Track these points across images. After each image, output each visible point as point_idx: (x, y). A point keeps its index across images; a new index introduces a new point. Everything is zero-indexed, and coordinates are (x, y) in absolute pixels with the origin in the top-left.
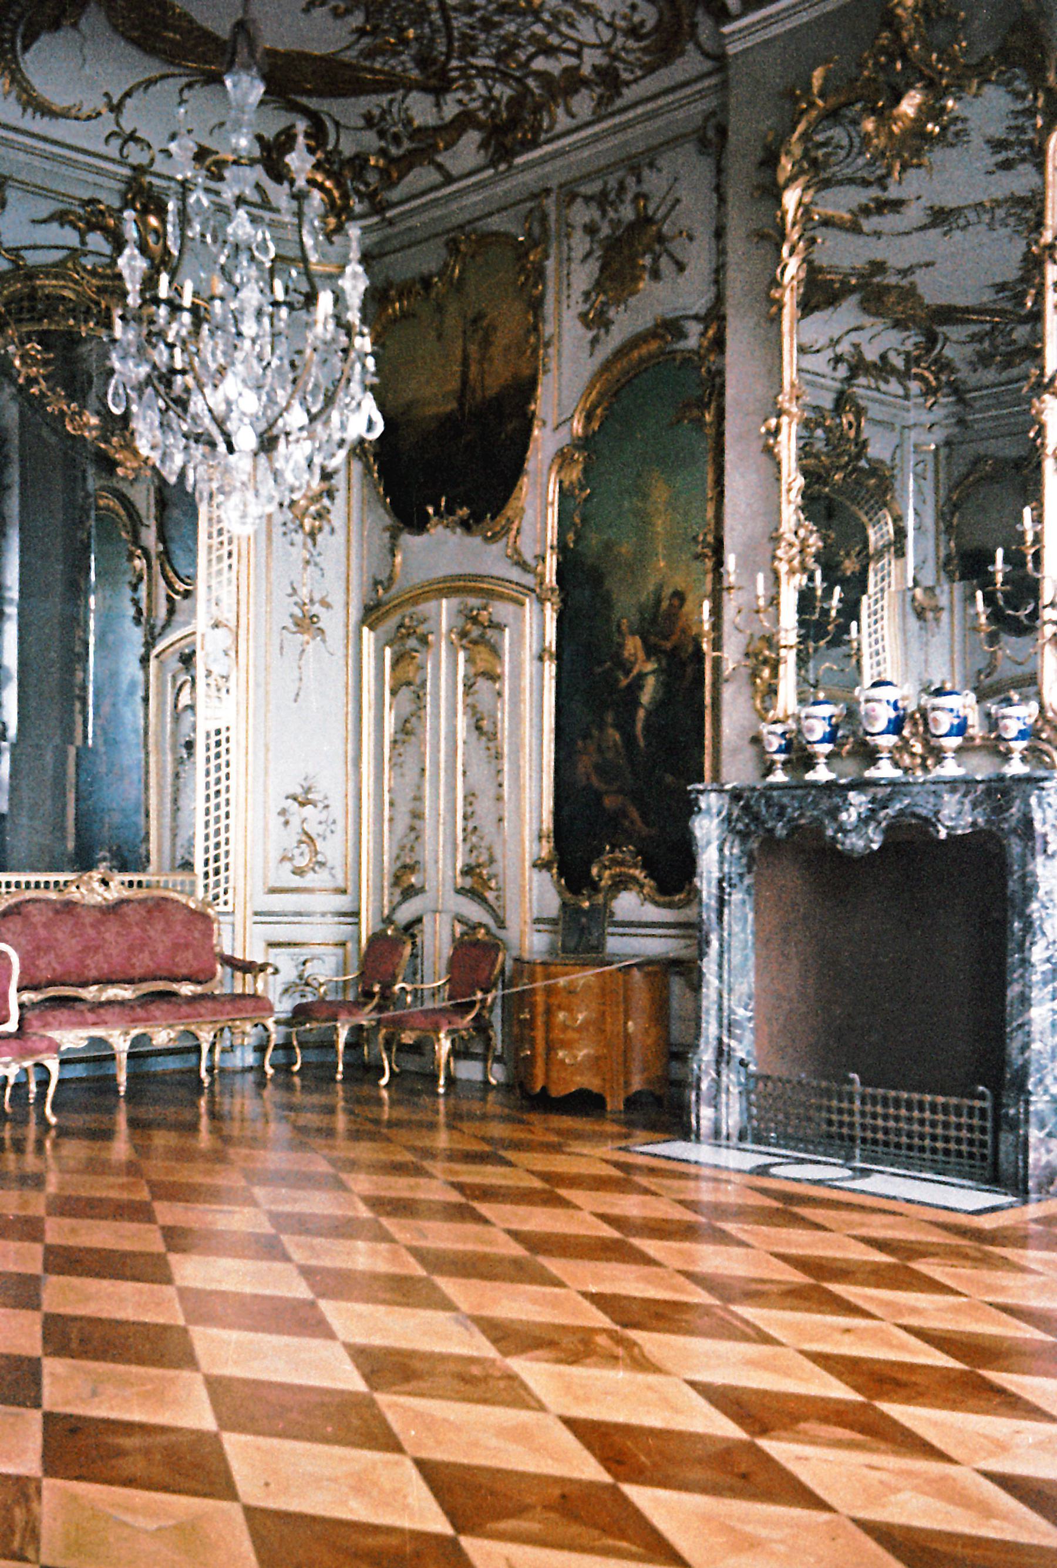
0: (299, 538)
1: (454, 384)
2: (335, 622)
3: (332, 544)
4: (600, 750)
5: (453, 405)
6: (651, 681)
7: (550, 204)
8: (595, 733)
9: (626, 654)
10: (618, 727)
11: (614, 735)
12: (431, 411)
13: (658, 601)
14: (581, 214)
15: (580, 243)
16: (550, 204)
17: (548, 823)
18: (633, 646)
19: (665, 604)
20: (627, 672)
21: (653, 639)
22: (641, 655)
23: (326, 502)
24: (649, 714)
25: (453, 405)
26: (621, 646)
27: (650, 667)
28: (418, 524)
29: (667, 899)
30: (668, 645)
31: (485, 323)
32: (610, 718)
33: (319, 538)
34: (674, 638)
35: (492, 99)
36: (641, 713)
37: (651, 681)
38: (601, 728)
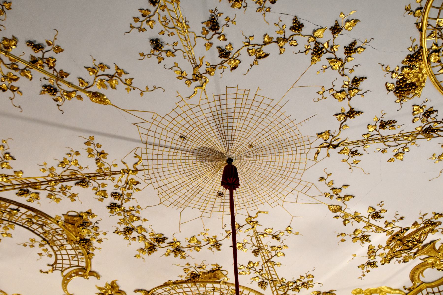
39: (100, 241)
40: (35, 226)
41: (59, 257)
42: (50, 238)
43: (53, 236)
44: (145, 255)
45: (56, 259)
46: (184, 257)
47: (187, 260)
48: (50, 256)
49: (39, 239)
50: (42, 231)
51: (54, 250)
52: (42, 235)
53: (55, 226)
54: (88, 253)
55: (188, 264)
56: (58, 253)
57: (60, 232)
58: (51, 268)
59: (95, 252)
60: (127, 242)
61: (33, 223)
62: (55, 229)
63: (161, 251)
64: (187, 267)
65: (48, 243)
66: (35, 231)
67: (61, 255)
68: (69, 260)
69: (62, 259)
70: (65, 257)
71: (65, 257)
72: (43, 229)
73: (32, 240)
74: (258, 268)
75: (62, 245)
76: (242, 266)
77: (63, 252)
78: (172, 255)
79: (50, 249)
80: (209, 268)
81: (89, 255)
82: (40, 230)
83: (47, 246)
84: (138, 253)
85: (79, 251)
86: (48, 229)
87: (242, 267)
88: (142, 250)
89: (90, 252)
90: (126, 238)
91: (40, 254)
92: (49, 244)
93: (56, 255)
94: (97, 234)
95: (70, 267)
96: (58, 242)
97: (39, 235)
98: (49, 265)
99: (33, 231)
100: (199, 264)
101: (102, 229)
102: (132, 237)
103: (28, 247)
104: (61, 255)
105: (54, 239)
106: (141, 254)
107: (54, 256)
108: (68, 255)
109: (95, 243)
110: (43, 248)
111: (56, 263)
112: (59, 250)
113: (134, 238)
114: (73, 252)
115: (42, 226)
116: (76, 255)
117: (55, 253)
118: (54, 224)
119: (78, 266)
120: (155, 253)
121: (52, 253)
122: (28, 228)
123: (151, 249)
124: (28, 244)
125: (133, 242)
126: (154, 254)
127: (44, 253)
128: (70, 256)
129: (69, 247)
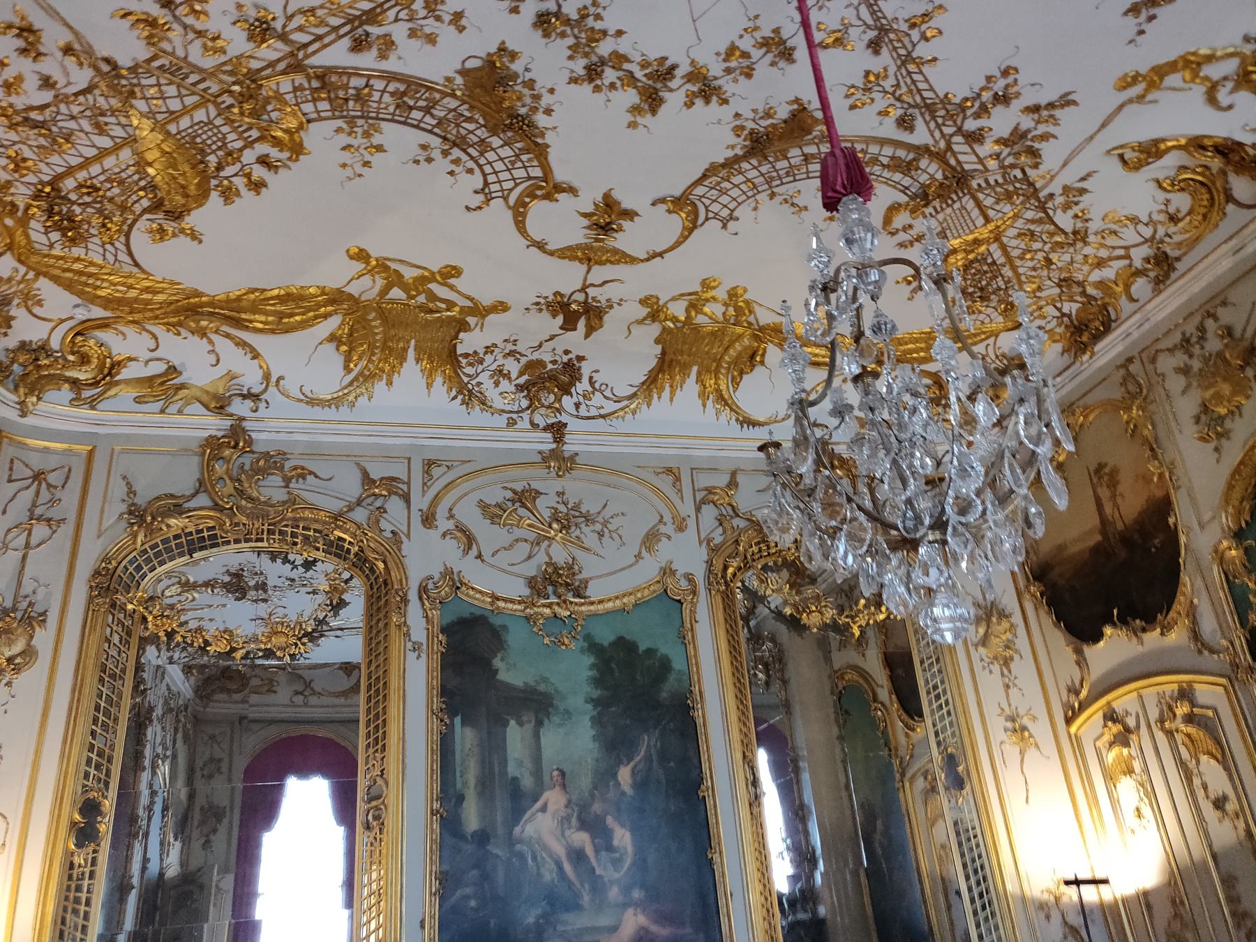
0: (996, 668)
1: (1097, 521)
2: (1040, 730)
3: (1023, 668)
5: (1099, 538)
7: (1135, 368)
12: (1073, 549)
14: (1167, 363)
15: (1176, 383)
16: (1135, 368)
23: (1009, 635)
25: (1099, 538)
28: (1097, 637)
31: (1107, 470)
33: (1012, 665)
35: (1064, 315)
39: (548, 112)
40: (416, 115)
41: (488, 169)
42: (454, 132)
43: (458, 125)
44: (647, 119)
45: (485, 175)
46: (726, 102)
47: (735, 105)
48: (470, 171)
49: (435, 142)
50: (434, 122)
51: (472, 158)
52: (436, 130)
53: (453, 104)
54: (536, 144)
55: (737, 115)
56: (482, 161)
57: (467, 114)
58: (481, 197)
59: (549, 138)
60: (600, 97)
61: (411, 108)
62: (455, 110)
63: (674, 99)
64: (738, 123)
65: (455, 144)
66: (422, 125)
67: (490, 163)
68: (508, 170)
69: (496, 173)
70: (499, 166)
71: (499, 166)
72: (432, 116)
73: (424, 147)
74: (888, 84)
75: (483, 141)
76: (853, 87)
77: (491, 156)
78: (699, 102)
79: (464, 157)
80: (783, 113)
81: (541, 153)
82: (428, 119)
83: (456, 153)
84: (630, 118)
85: (519, 145)
86: (442, 114)
87: (852, 90)
88: (635, 110)
89: (539, 141)
90: (597, 89)
91: (451, 173)
92: (458, 146)
93: (480, 166)
94: (537, 98)
95: (517, 185)
96: (471, 136)
97: (430, 132)
98: (476, 192)
99: (417, 127)
100: (761, 109)
101: (542, 84)
102: (607, 82)
103: (423, 163)
104: (490, 163)
105: (463, 132)
106: (639, 119)
107: (477, 170)
108: (502, 159)
109: (541, 120)
110: (450, 158)
111: (486, 184)
112: (482, 154)
113: (612, 86)
114: (506, 152)
115: (427, 110)
116: (517, 156)
117: (476, 162)
118: (447, 100)
119: (529, 178)
120: (663, 106)
121: (471, 164)
122: (405, 123)
123: (652, 101)
124: (421, 158)
125: (613, 95)
126: (663, 110)
127: (457, 169)
128: (506, 161)
129: (496, 142)
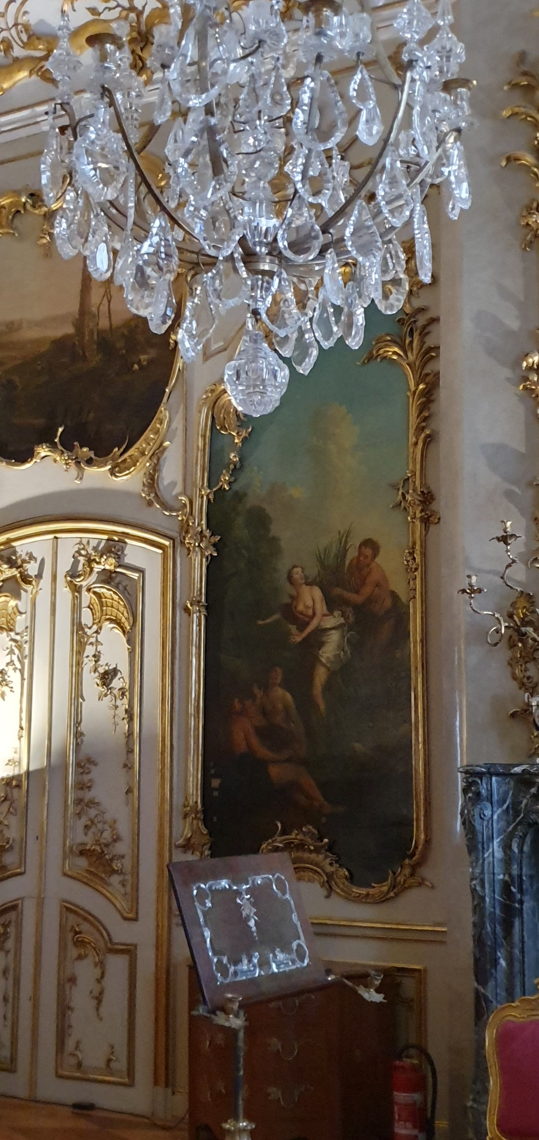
4: (264, 713)
6: (334, 638)
8: (258, 692)
9: (301, 607)
10: (286, 685)
11: (282, 696)
13: (343, 552)
17: (195, 796)
18: (312, 598)
19: (352, 554)
20: (302, 626)
21: (338, 591)
22: (321, 607)
24: (332, 674)
26: (294, 598)
27: (330, 622)
29: (363, 891)
30: (358, 599)
32: (278, 675)
34: (367, 591)
36: (321, 675)
37: (334, 638)
38: (266, 688)
